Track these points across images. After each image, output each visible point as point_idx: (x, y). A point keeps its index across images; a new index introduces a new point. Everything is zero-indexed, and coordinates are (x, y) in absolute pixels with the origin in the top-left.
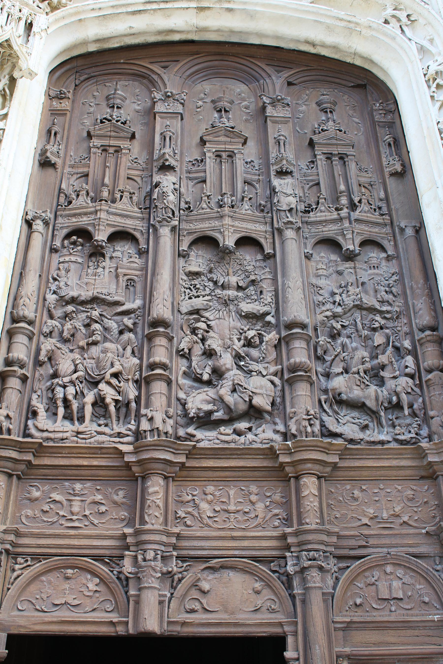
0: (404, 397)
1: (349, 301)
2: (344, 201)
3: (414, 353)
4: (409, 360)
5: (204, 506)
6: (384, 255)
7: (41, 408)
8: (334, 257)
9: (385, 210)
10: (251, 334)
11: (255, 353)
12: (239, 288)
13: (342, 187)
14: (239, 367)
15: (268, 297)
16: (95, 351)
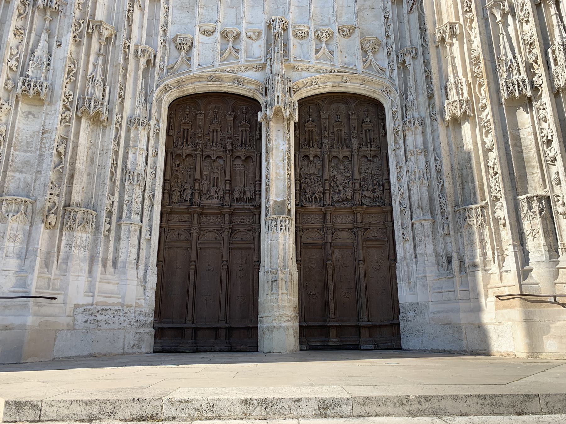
0: (380, 196)
1: (369, 173)
2: (369, 145)
3: (383, 185)
4: (381, 187)
5: (338, 219)
6: (378, 159)
7: (304, 200)
8: (366, 160)
9: (379, 147)
10: (347, 181)
11: (347, 185)
12: (343, 169)
13: (369, 141)
14: (344, 189)
15: (350, 172)
16: (313, 186)
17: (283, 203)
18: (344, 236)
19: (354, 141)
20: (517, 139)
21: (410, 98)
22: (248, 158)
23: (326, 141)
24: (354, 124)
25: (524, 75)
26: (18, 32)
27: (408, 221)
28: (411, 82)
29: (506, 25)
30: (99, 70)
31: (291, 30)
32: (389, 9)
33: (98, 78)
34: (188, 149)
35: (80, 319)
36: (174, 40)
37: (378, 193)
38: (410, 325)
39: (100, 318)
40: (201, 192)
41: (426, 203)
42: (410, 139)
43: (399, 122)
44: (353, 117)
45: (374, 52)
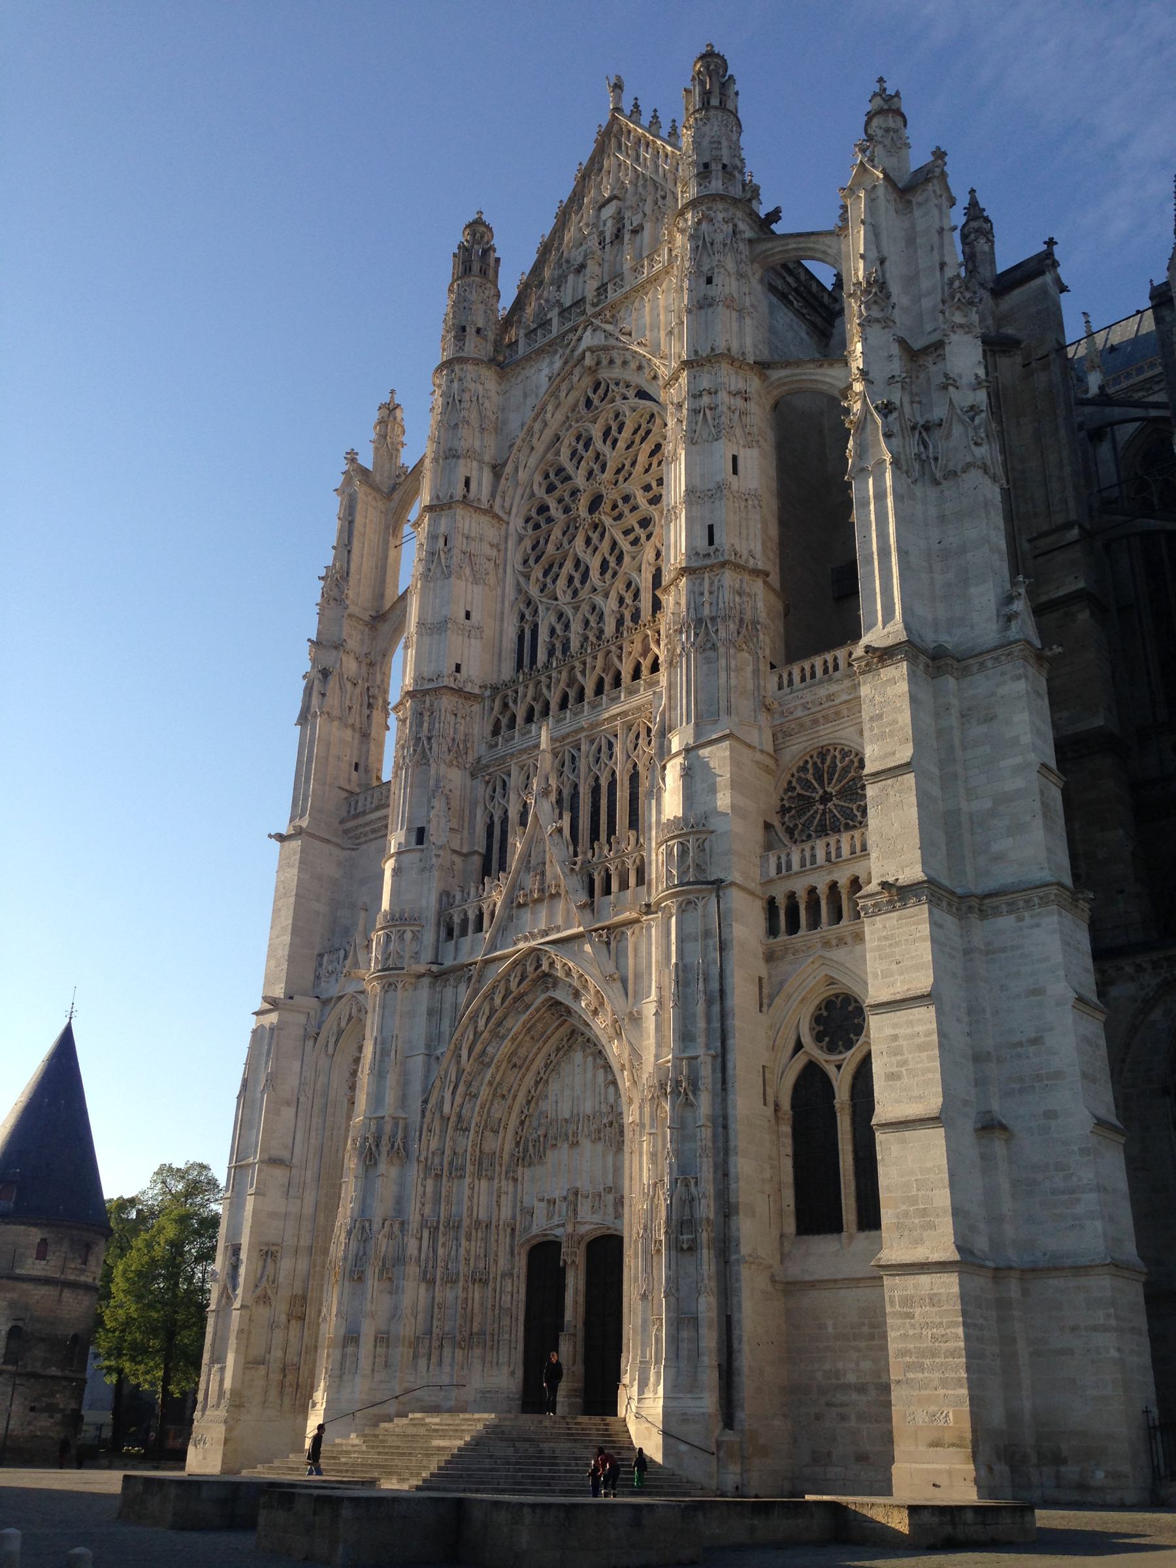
26: (444, 1245)
30: (482, 1250)
33: (482, 1256)
35: (478, 1395)
39: (487, 1395)
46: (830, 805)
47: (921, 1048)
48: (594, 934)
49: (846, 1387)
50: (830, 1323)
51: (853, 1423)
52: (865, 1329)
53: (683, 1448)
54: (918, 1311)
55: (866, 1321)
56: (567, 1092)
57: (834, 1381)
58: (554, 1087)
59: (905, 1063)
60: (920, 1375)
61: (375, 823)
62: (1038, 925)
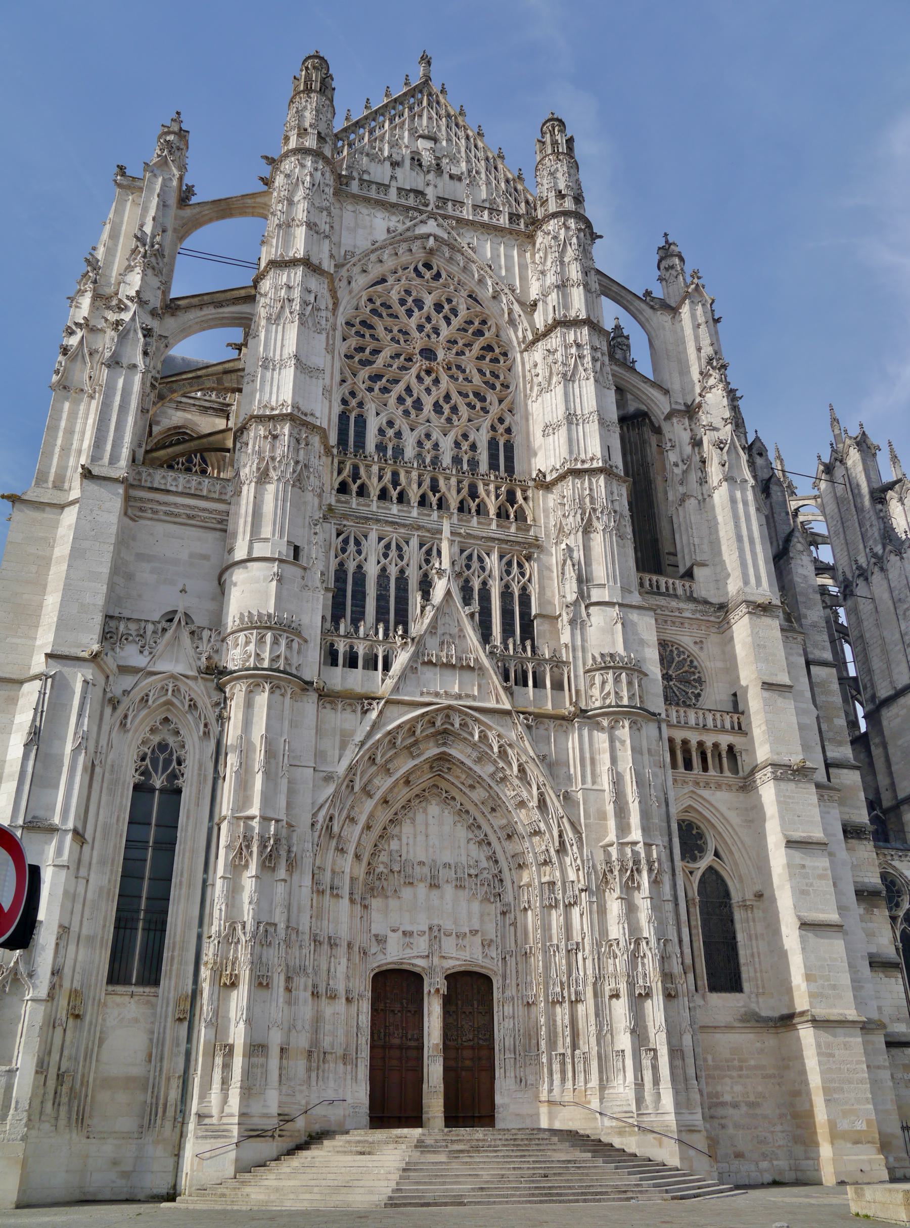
17: (437, 1045)
18: (468, 1063)
19: (475, 1002)
20: (555, 1021)
21: (507, 981)
22: (416, 1012)
23: (459, 1002)
24: (475, 991)
25: (559, 990)
27: (502, 1057)
28: (508, 972)
29: (555, 955)
31: (442, 931)
32: (499, 918)
34: (382, 1006)
35: (352, 1110)
36: (376, 936)
37: (487, 1036)
38: (500, 1115)
40: (390, 1034)
41: (512, 1047)
42: (506, 1008)
43: (500, 995)
44: (475, 987)
45: (489, 946)
46: (671, 683)
47: (821, 877)
48: (522, 716)
49: (723, 1104)
50: (710, 1058)
51: (731, 1130)
52: (736, 1063)
53: (692, 1152)
54: (837, 1053)
55: (736, 1057)
56: (421, 838)
57: (715, 1100)
58: (407, 829)
59: (812, 885)
60: (841, 1096)
61: (144, 502)
62: (829, 813)
